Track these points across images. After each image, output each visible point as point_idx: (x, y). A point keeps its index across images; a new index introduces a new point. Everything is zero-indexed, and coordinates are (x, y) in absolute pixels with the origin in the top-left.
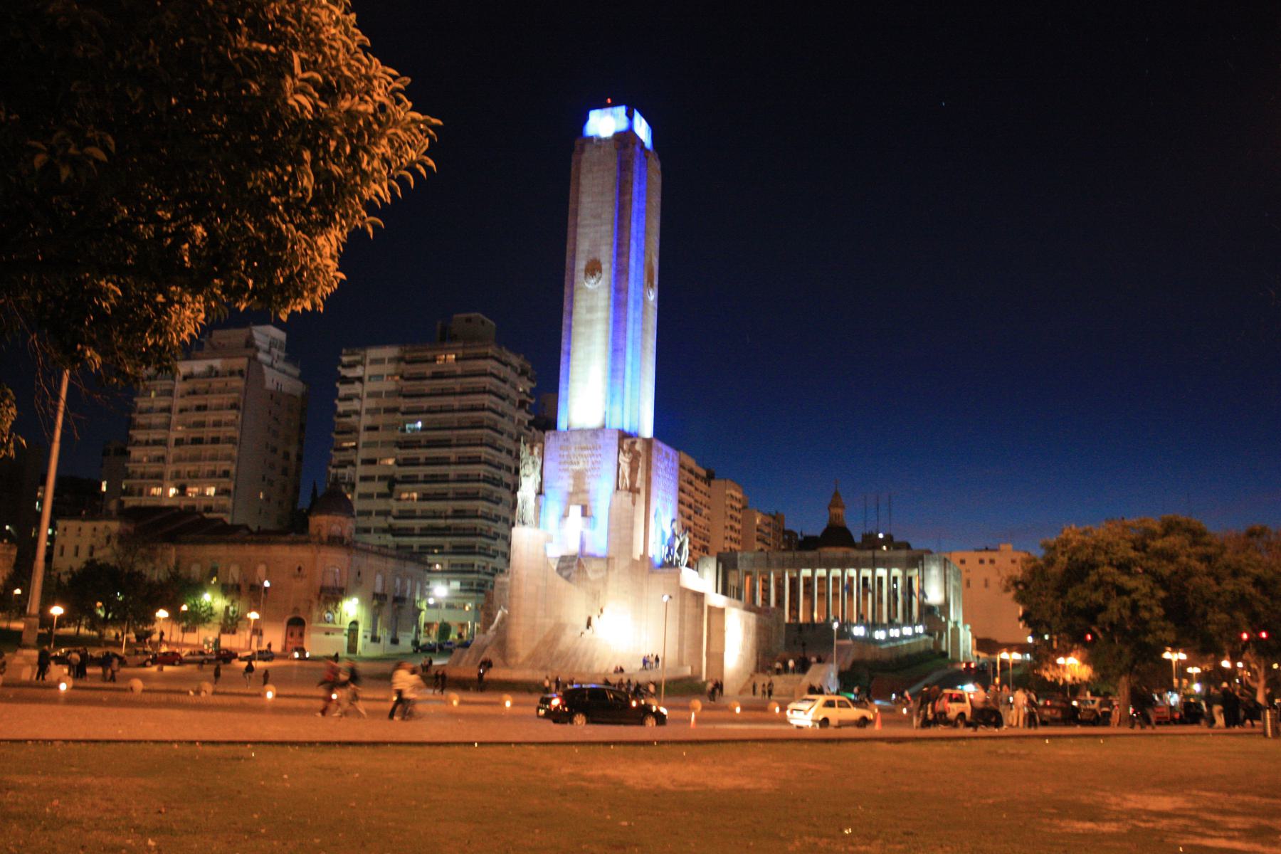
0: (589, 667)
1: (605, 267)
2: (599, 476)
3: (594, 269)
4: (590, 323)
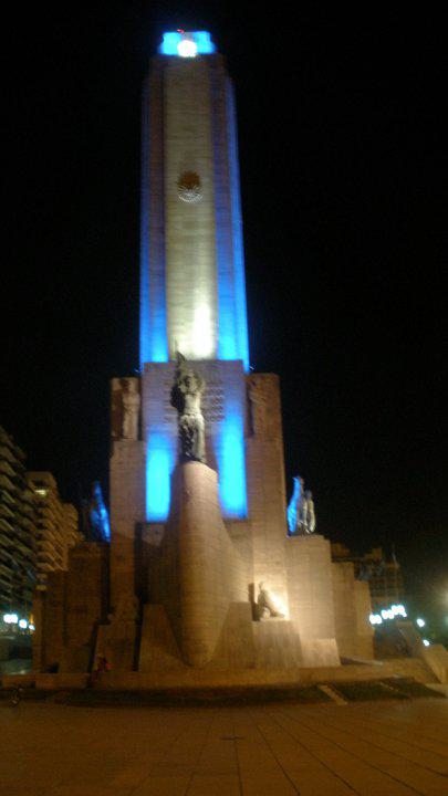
0: (300, 658)
1: (205, 180)
2: (222, 417)
3: (190, 181)
4: (190, 240)
